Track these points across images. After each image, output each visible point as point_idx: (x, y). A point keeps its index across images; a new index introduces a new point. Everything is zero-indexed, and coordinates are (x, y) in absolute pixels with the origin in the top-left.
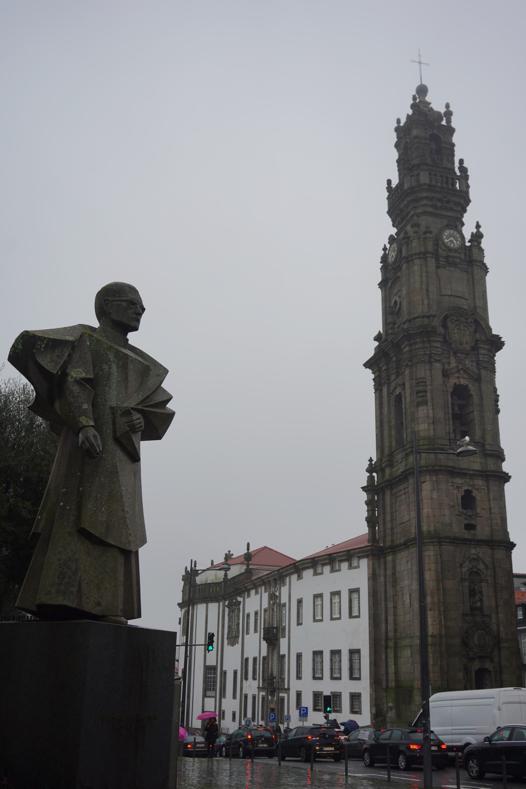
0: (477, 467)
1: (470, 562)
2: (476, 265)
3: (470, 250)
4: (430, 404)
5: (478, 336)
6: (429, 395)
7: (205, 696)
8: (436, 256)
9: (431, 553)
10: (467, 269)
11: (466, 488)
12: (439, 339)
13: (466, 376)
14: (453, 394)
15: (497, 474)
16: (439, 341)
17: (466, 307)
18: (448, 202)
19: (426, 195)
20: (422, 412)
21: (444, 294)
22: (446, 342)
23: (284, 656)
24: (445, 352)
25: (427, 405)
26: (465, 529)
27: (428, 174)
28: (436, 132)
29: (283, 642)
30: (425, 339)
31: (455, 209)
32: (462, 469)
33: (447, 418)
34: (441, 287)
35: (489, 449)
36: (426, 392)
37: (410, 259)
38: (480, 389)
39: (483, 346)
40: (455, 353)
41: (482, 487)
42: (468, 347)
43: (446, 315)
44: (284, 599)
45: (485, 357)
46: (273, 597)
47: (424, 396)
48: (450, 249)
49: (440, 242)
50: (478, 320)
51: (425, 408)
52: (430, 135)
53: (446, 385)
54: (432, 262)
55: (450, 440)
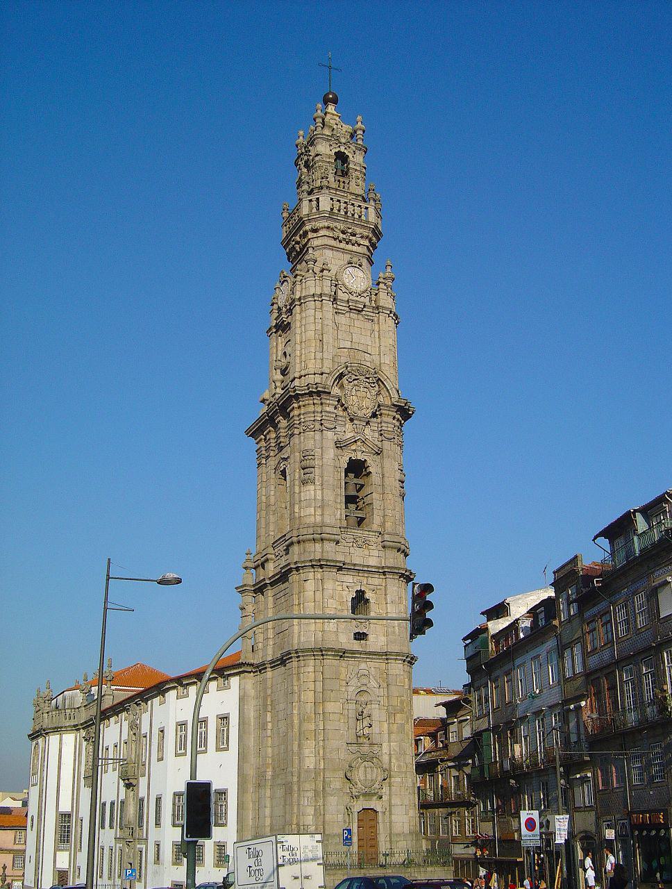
0: (373, 562)
1: (358, 679)
4: (317, 483)
5: (381, 399)
6: (317, 471)
7: (57, 849)
9: (311, 669)
14: (347, 471)
16: (333, 405)
17: (368, 364)
18: (354, 235)
19: (326, 224)
20: (310, 491)
23: (142, 800)
26: (355, 639)
28: (342, 149)
29: (143, 782)
32: (355, 565)
40: (352, 420)
41: (379, 587)
44: (145, 729)
45: (389, 425)
46: (134, 727)
51: (312, 487)
54: (328, 305)
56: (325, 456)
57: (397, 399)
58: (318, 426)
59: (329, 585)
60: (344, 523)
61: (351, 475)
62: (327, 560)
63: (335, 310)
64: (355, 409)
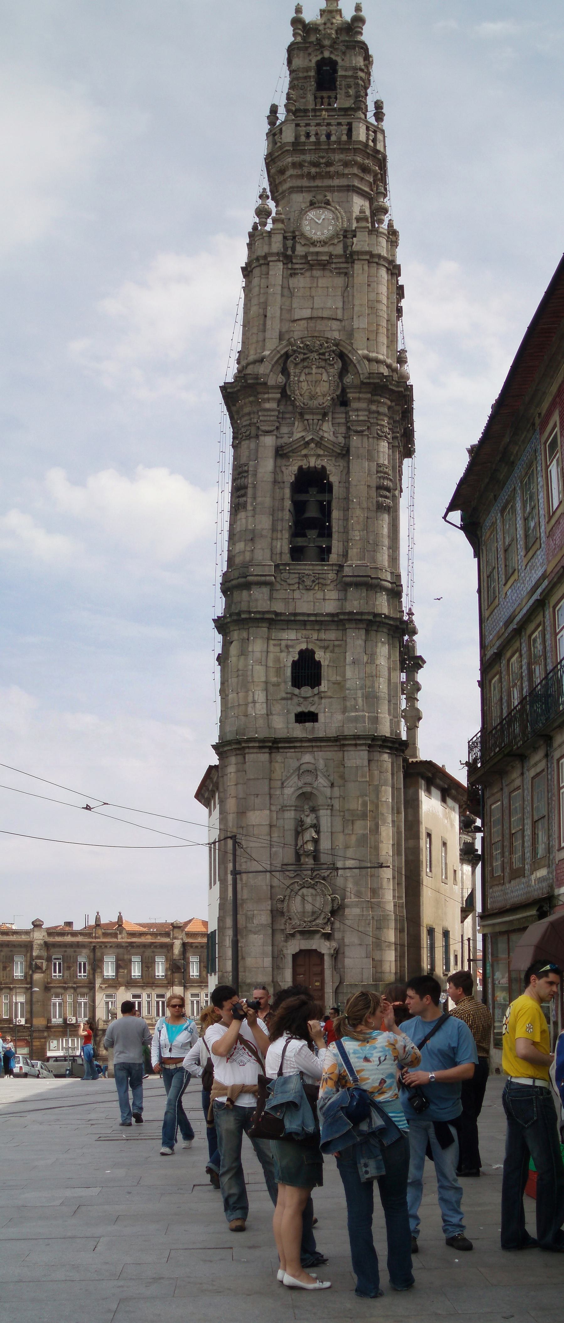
0: (330, 607)
2: (358, 259)
8: (287, 258)
10: (347, 268)
12: (271, 396)
13: (321, 452)
16: (273, 399)
18: (329, 164)
19: (290, 160)
21: (296, 318)
24: (287, 416)
25: (246, 510)
31: (346, 171)
32: (295, 614)
33: (279, 528)
34: (294, 306)
37: (249, 269)
38: (348, 471)
39: (357, 395)
40: (301, 415)
43: (286, 353)
45: (360, 413)
47: (243, 496)
48: (313, 244)
49: (297, 233)
50: (346, 352)
51: (242, 515)
55: (277, 566)
56: (261, 470)
57: (367, 375)
58: (254, 432)
60: (287, 558)
61: (313, 491)
62: (250, 612)
63: (290, 272)
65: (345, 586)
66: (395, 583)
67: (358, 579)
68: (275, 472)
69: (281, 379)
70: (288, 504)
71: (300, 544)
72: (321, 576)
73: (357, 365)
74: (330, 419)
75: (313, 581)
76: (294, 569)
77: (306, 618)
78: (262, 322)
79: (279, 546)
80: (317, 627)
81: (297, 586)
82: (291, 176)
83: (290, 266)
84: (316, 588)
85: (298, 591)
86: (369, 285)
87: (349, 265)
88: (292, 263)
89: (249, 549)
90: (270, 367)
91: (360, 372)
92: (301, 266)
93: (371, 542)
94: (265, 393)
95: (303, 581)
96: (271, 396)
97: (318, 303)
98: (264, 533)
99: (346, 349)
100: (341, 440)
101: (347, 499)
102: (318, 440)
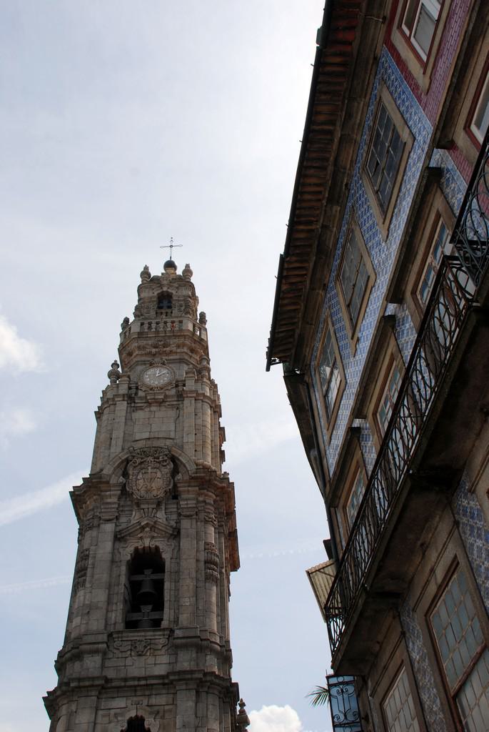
2: (187, 397)
3: (184, 385)
4: (88, 585)
6: (89, 572)
8: (130, 399)
11: (133, 714)
13: (156, 535)
15: (189, 676)
16: (115, 495)
18: (165, 346)
19: (136, 344)
22: (124, 492)
24: (126, 509)
27: (139, 324)
28: (165, 289)
30: (95, 497)
31: (178, 351)
32: (125, 680)
33: (115, 601)
35: (181, 636)
36: (86, 569)
40: (138, 505)
41: (167, 708)
42: (161, 494)
45: (189, 502)
47: (82, 576)
50: (177, 455)
52: (158, 294)
53: (120, 553)
54: (122, 406)
55: (110, 635)
57: (195, 470)
58: (96, 522)
59: (84, 718)
60: (121, 627)
61: (148, 572)
62: (79, 680)
64: (143, 492)
65: (176, 648)
66: (224, 646)
67: (189, 640)
68: (113, 553)
69: (122, 479)
70: (123, 579)
71: (134, 619)
72: (153, 641)
73: (187, 465)
74: (164, 508)
75: (145, 647)
76: (128, 637)
77: (136, 683)
78: (108, 443)
79: (113, 617)
80: (147, 693)
81: (129, 652)
82: (137, 355)
83: (133, 405)
84: (148, 654)
85: (130, 658)
86: (196, 415)
87: (180, 402)
88: (135, 402)
89: (85, 622)
90: (112, 469)
91: (189, 469)
92: (142, 405)
93: (200, 608)
94: (106, 491)
95: (136, 647)
96: (112, 493)
97: (154, 428)
98: (100, 605)
99: (177, 453)
100: (173, 523)
101: (178, 572)
102: (152, 523)
